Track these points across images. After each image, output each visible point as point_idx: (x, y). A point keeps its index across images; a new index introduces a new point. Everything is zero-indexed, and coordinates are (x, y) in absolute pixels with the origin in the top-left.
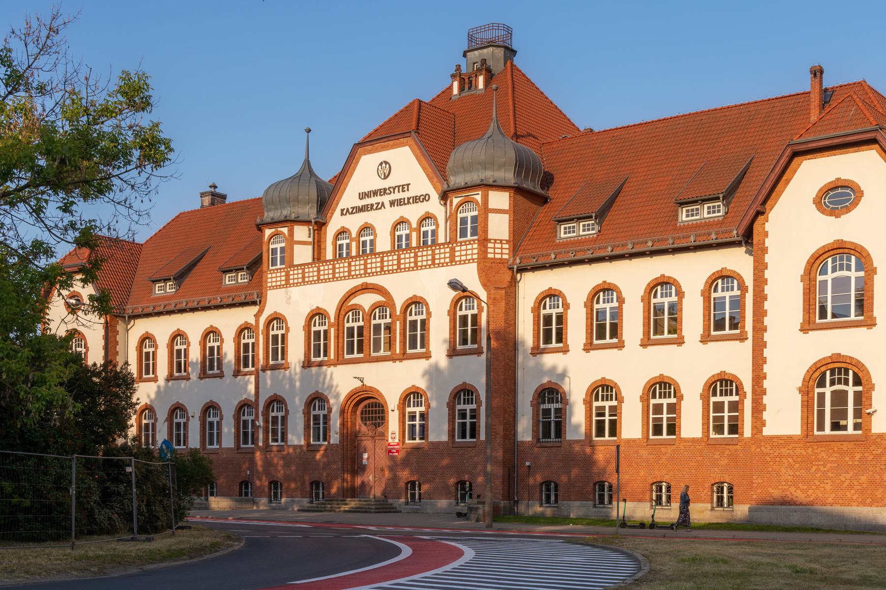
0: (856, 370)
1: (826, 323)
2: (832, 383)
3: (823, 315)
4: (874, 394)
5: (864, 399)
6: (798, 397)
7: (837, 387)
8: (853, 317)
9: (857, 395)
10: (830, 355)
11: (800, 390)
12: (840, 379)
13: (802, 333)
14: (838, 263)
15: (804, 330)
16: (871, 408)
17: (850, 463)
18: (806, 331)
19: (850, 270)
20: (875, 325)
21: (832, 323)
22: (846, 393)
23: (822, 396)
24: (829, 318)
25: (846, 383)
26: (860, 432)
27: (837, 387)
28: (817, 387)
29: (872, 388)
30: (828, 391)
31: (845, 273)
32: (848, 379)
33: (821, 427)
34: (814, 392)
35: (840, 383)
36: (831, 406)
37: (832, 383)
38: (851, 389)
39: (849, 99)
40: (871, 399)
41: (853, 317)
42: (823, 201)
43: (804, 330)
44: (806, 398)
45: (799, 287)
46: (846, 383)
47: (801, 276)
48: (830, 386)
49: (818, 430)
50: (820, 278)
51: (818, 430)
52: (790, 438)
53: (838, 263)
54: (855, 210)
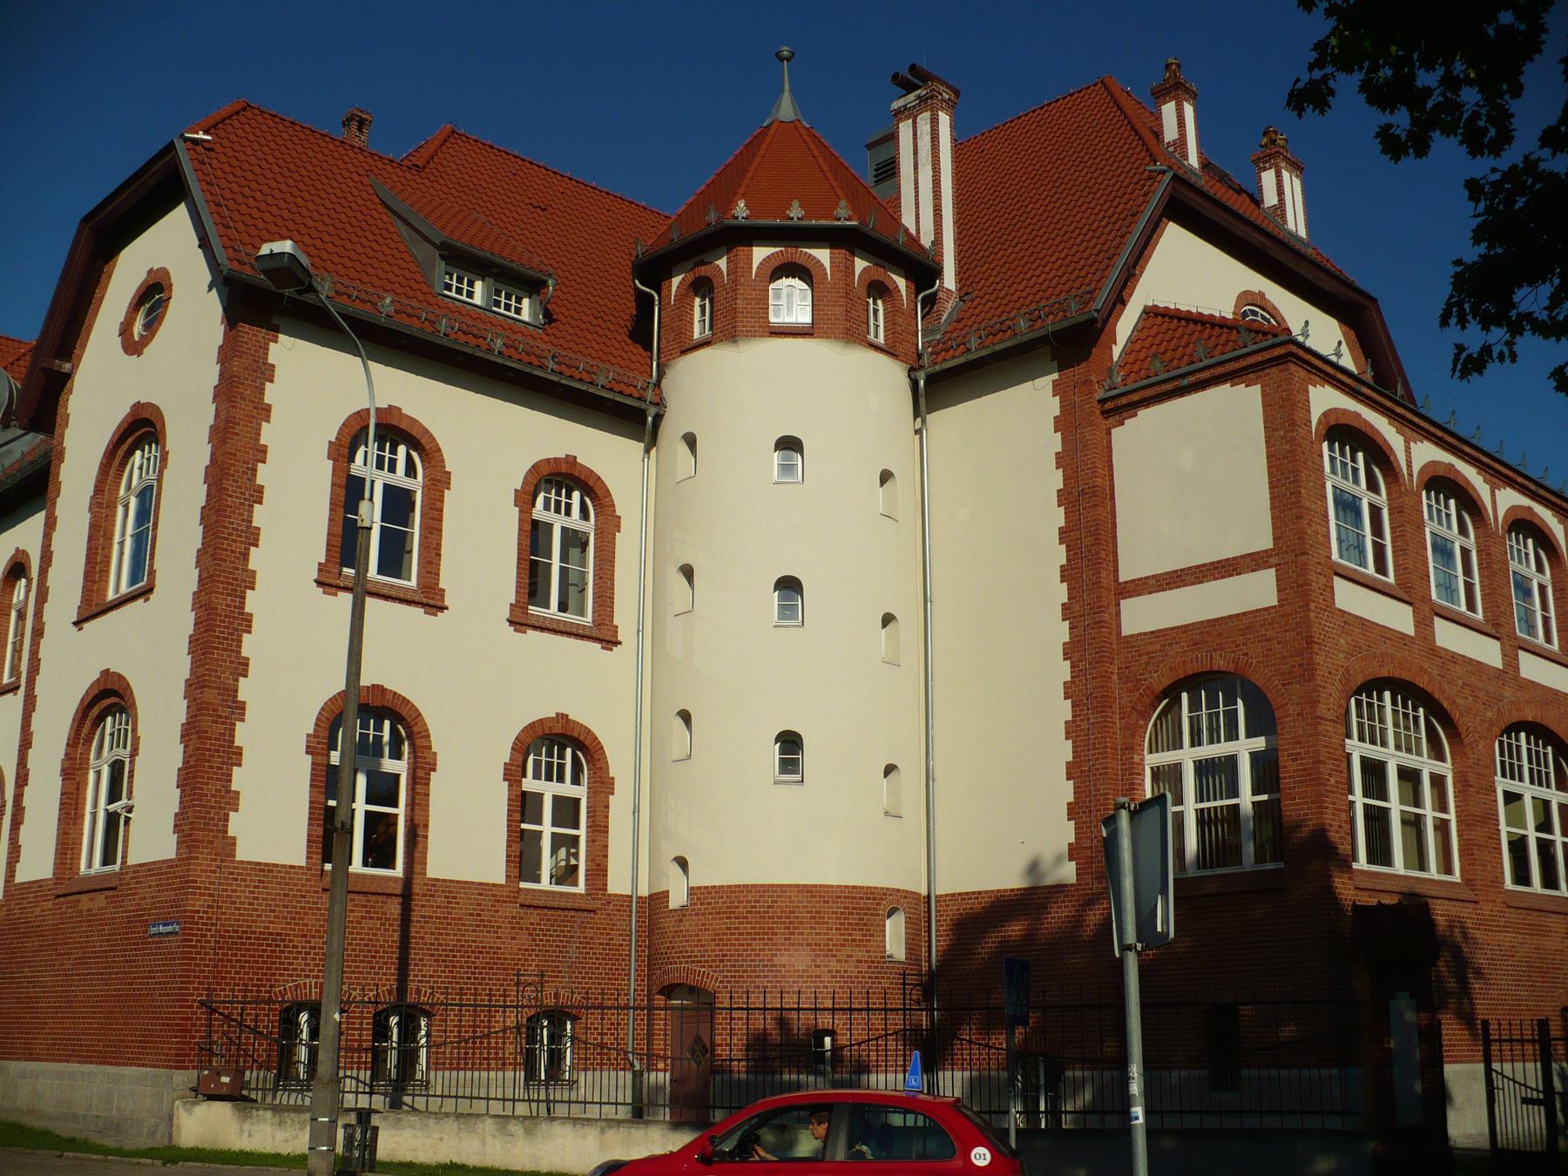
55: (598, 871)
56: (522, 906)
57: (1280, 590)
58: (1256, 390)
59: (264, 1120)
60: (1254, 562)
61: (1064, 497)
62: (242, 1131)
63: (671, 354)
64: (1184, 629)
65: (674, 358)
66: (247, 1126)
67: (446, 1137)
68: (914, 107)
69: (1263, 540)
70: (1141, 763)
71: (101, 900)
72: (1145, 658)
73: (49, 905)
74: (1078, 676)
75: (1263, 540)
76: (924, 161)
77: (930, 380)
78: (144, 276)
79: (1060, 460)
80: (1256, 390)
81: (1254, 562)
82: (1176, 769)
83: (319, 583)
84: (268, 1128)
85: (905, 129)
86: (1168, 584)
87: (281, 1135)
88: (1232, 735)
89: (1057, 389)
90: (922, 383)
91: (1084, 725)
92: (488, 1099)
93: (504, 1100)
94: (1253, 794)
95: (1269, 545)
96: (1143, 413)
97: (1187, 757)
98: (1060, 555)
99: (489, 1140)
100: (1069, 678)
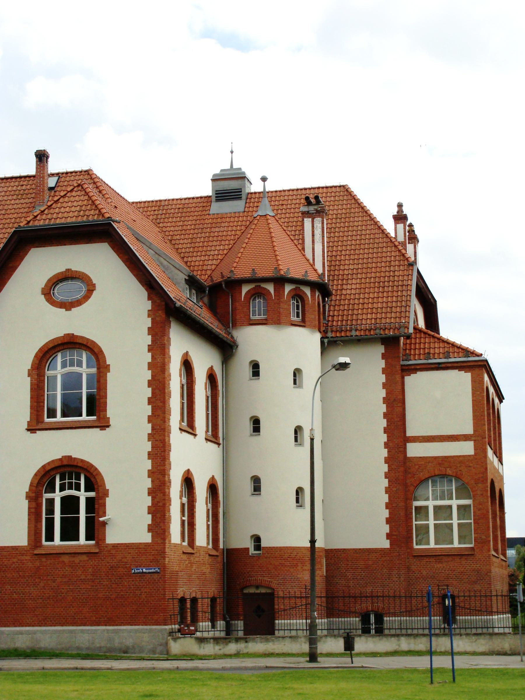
0: (88, 475)
1: (55, 423)
2: (62, 489)
3: (52, 413)
4: (108, 501)
5: (96, 506)
6: (25, 504)
7: (67, 492)
8: (84, 417)
9: (88, 499)
10: (61, 457)
11: (28, 497)
12: (70, 484)
13: (29, 432)
14: (68, 358)
15: (31, 429)
16: (105, 516)
17: (83, 577)
18: (34, 431)
19: (81, 366)
20: (108, 426)
21: (62, 422)
22: (78, 498)
23: (51, 502)
24: (59, 418)
25: (78, 488)
26: (93, 542)
27: (67, 492)
28: (45, 493)
29: (106, 493)
30: (57, 496)
31: (76, 369)
32: (80, 483)
33: (50, 537)
34: (42, 497)
35: (70, 488)
36: (62, 514)
37: (62, 489)
38: (83, 495)
39: (80, 188)
40: (104, 505)
41: (84, 417)
42: (52, 292)
43: (31, 429)
44: (34, 505)
45: (27, 382)
46: (78, 488)
47: (29, 370)
48: (80, 491)
49: (47, 540)
50: (49, 373)
51: (47, 540)
52: (15, 548)
53: (68, 358)
54: (87, 303)
55: (216, 541)
56: (210, 555)
57: (475, 449)
58: (470, 374)
59: (210, 643)
60: (465, 438)
61: (385, 400)
62: (200, 647)
63: (243, 323)
64: (435, 458)
65: (245, 325)
66: (202, 645)
67: (286, 644)
68: (313, 213)
69: (469, 430)
70: (412, 505)
71: (85, 558)
72: (417, 467)
73: (28, 558)
74: (391, 471)
75: (469, 430)
76: (318, 240)
77: (329, 342)
78: (63, 270)
79: (384, 386)
80: (470, 374)
81: (465, 438)
82: (437, 509)
83: (180, 429)
84: (212, 645)
85: (308, 222)
86: (428, 440)
87: (217, 648)
88: (451, 498)
89: (384, 356)
90: (326, 344)
91: (394, 489)
92: (297, 630)
93: (303, 630)
94: (458, 520)
95: (471, 432)
96: (419, 374)
97: (431, 504)
98: (384, 423)
99: (303, 644)
100: (387, 471)
